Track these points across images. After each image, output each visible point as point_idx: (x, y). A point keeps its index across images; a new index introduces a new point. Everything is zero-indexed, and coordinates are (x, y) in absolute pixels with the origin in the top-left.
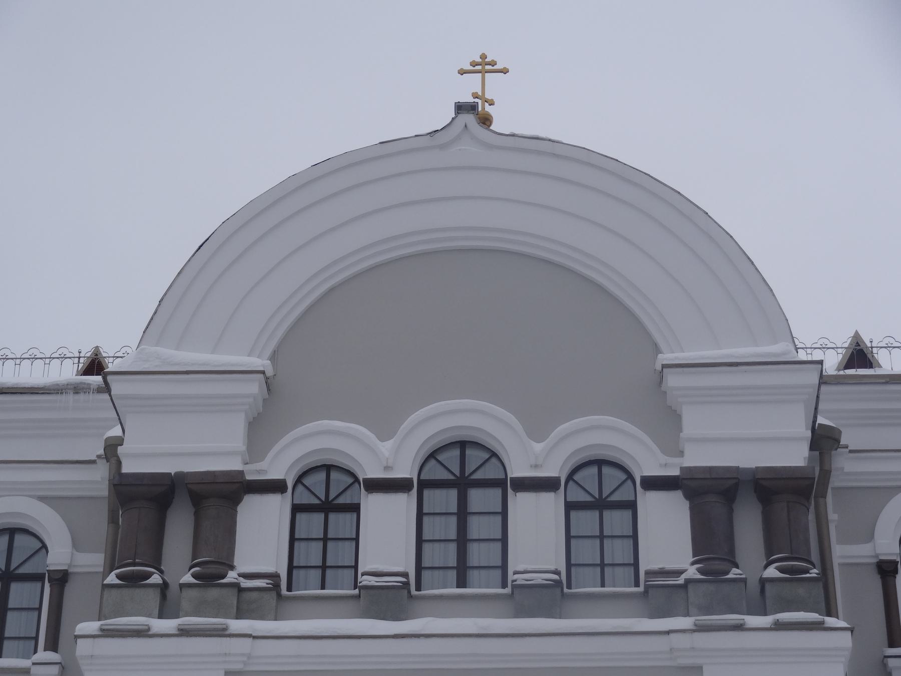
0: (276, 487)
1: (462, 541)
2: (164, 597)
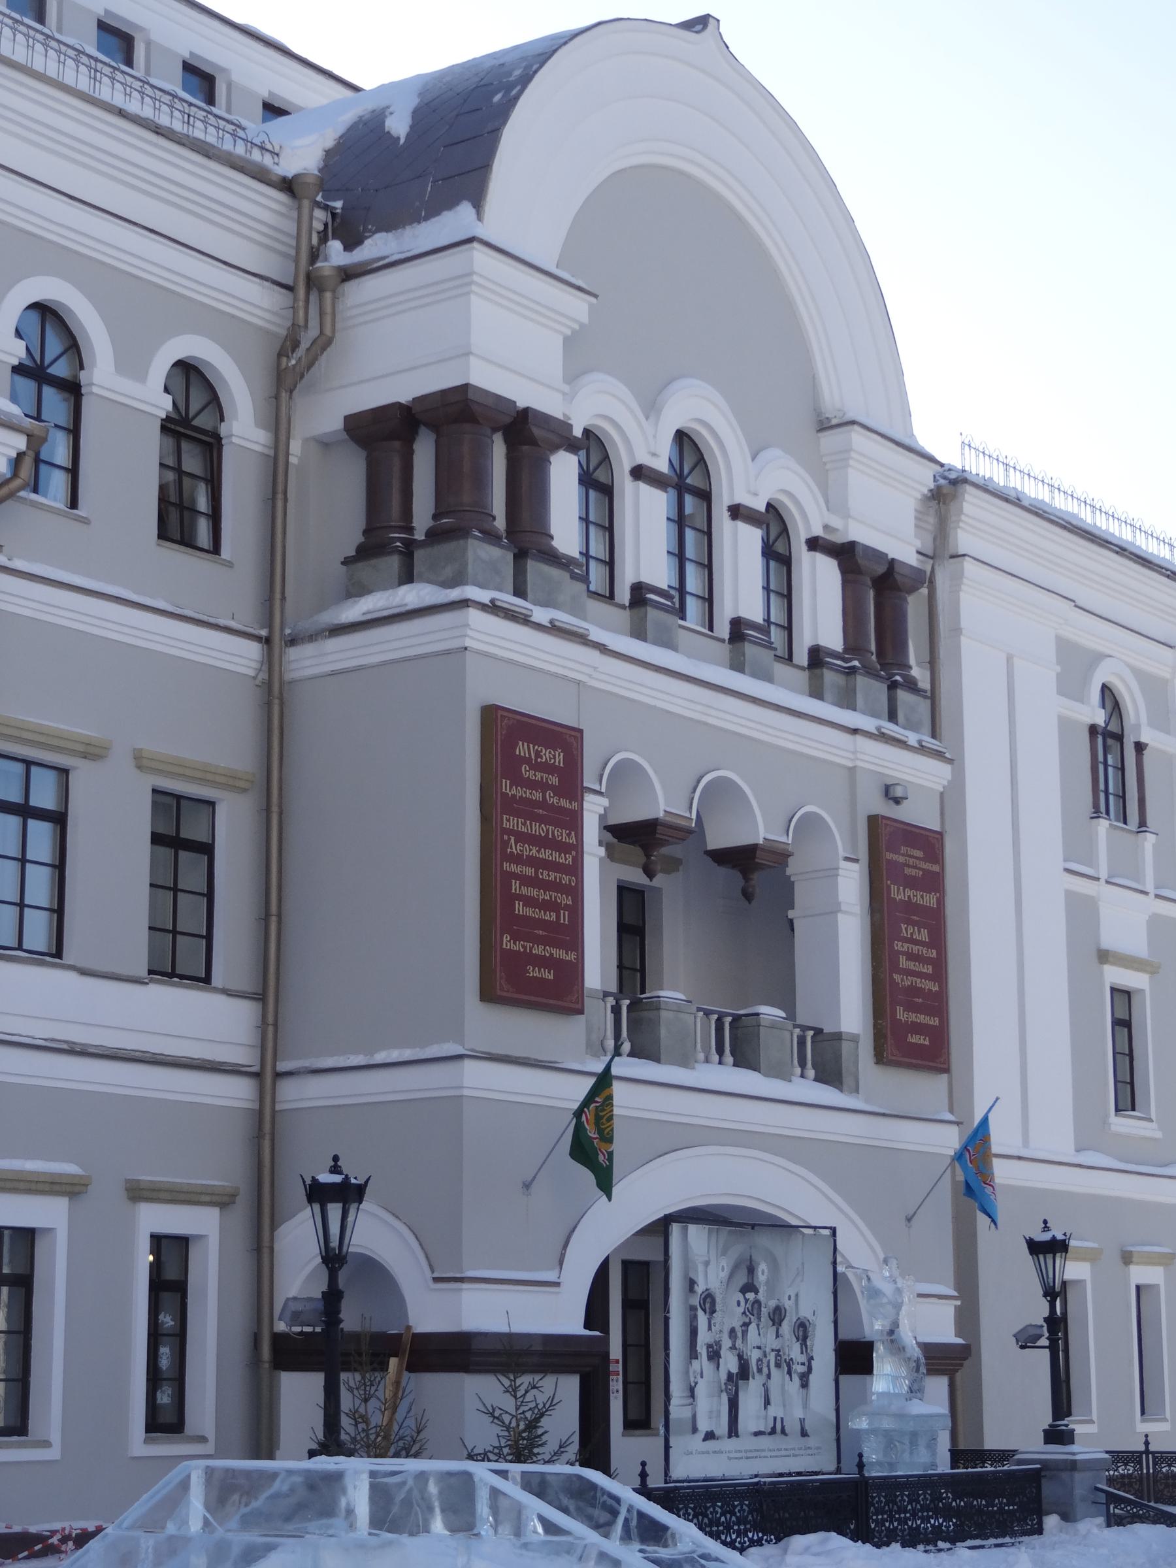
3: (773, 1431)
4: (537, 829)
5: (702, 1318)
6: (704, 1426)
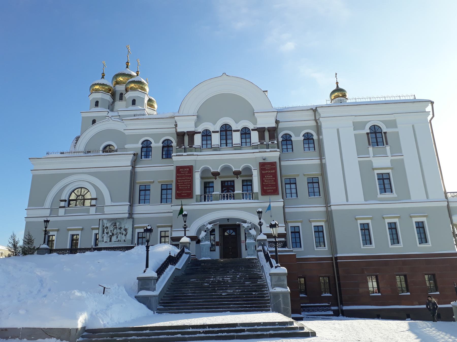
0: (199, 133)
1: (226, 140)
2: (185, 149)
3: (118, 241)
4: (183, 178)
5: (105, 230)
6: (105, 241)
